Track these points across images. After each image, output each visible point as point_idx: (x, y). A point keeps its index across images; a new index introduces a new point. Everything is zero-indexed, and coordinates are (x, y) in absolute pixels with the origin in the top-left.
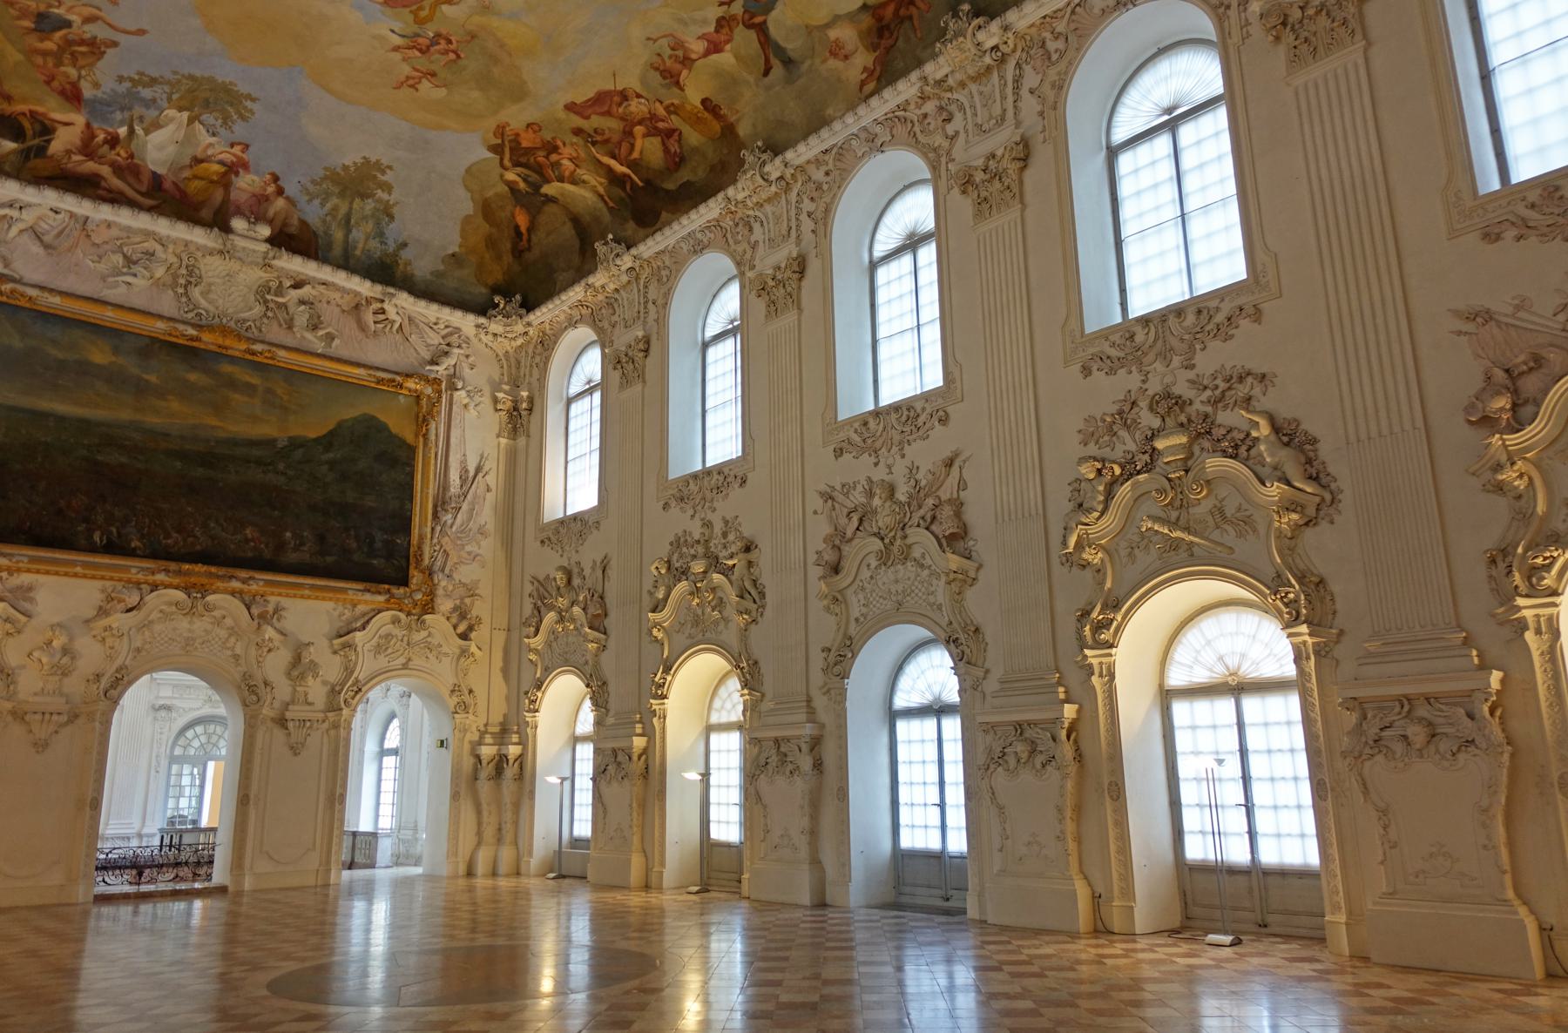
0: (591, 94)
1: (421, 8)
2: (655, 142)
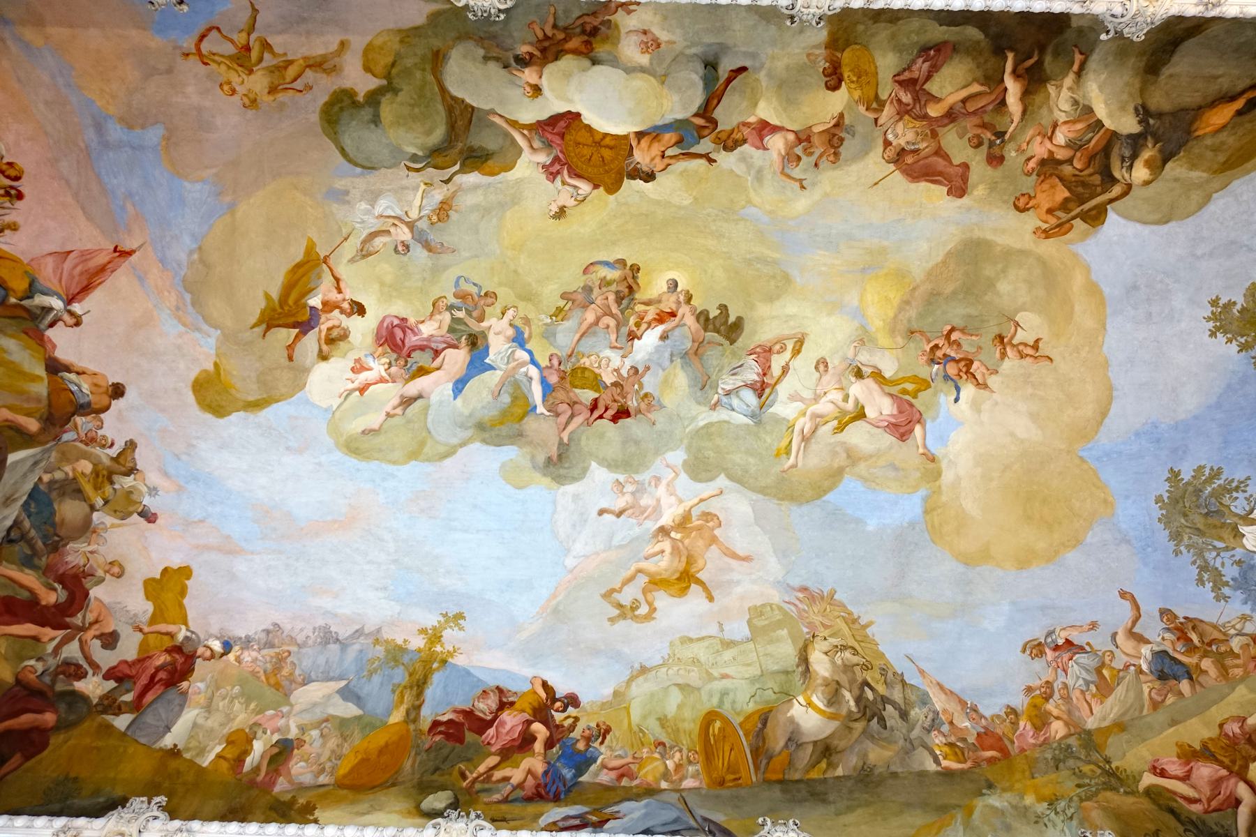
0: (923, 185)
1: (905, 392)
2: (933, 87)
